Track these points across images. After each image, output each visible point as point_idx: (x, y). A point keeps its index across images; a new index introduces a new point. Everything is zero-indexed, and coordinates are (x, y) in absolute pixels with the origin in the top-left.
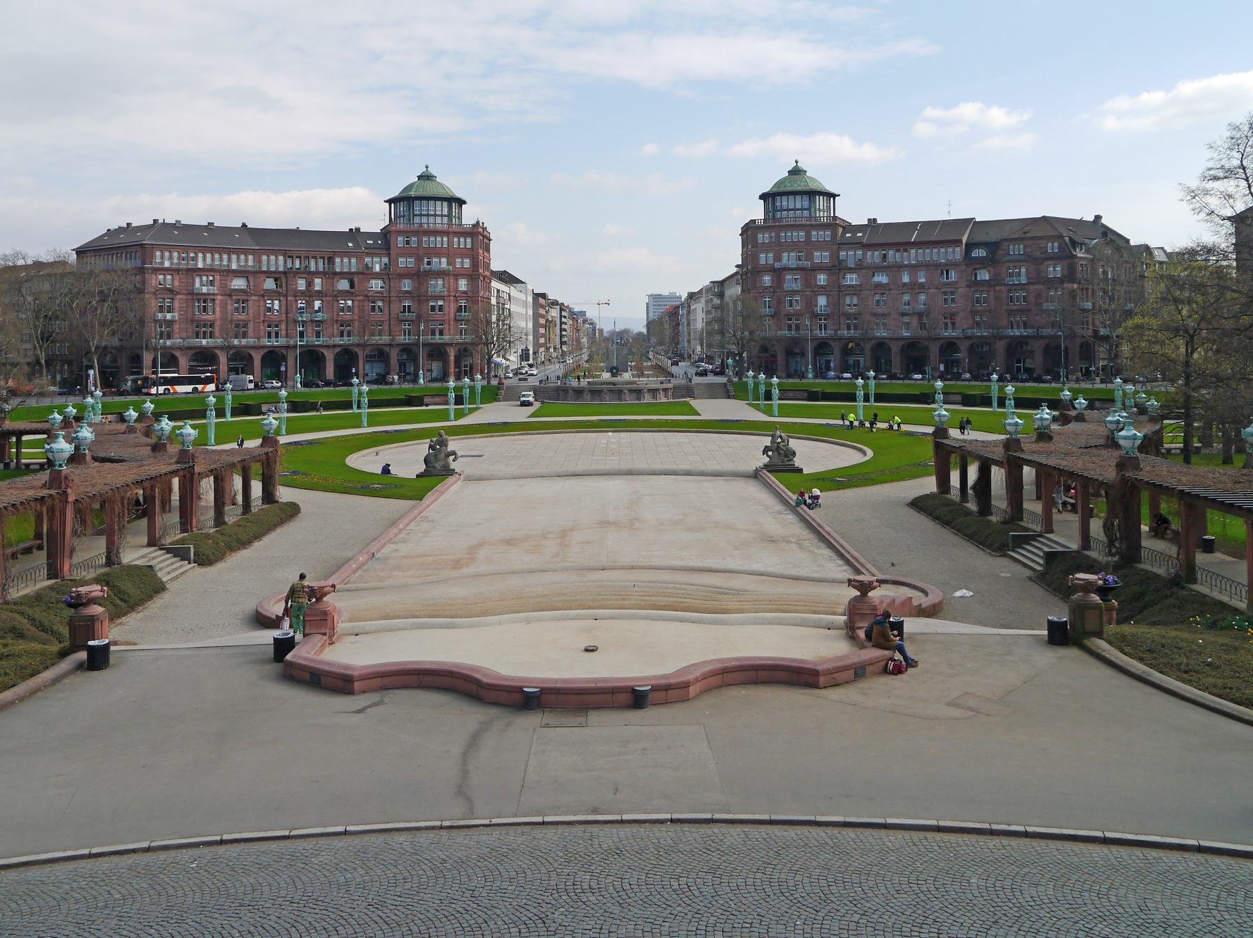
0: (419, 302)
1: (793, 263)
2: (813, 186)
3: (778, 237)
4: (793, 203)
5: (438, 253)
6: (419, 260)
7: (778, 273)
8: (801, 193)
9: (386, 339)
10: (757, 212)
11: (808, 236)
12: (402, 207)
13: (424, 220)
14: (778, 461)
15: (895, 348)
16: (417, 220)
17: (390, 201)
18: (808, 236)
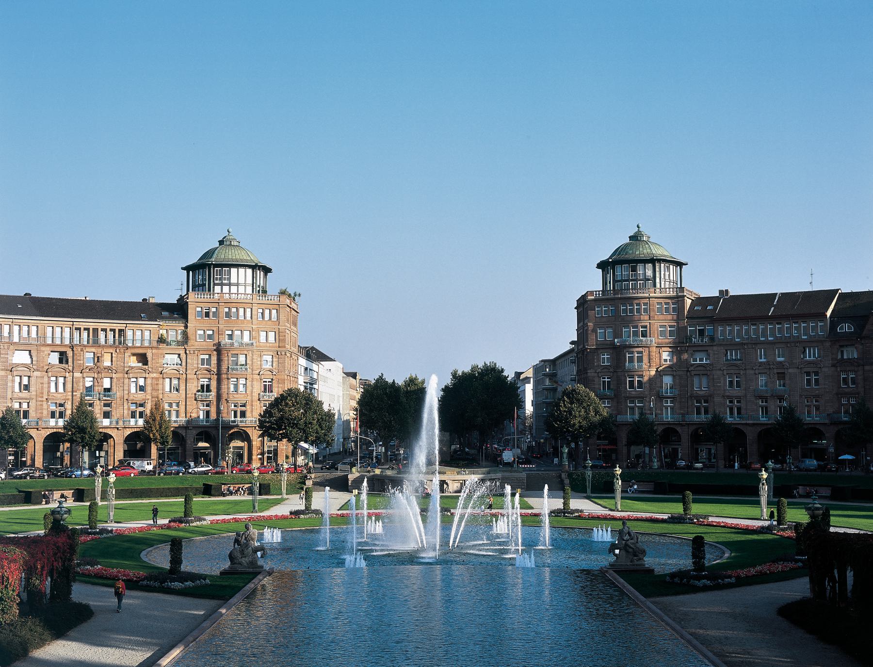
3: (617, 310)
10: (594, 282)
15: (751, 435)
17: (188, 269)
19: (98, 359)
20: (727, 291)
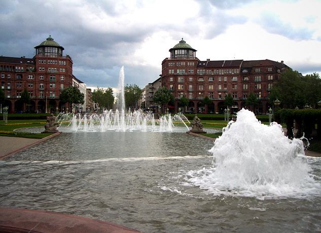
0: (46, 84)
1: (181, 74)
2: (189, 47)
3: (176, 64)
4: (181, 54)
5: (53, 66)
6: (47, 68)
7: (176, 76)
8: (184, 49)
9: (34, 97)
11: (186, 64)
12: (41, 50)
13: (49, 54)
14: (196, 129)
15: (216, 104)
16: (46, 54)
18: (186, 64)
19: (6, 76)
20: (209, 59)
